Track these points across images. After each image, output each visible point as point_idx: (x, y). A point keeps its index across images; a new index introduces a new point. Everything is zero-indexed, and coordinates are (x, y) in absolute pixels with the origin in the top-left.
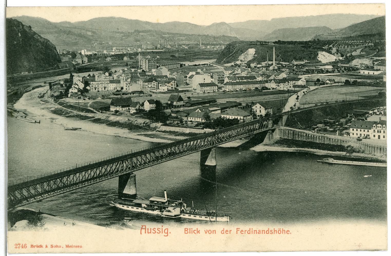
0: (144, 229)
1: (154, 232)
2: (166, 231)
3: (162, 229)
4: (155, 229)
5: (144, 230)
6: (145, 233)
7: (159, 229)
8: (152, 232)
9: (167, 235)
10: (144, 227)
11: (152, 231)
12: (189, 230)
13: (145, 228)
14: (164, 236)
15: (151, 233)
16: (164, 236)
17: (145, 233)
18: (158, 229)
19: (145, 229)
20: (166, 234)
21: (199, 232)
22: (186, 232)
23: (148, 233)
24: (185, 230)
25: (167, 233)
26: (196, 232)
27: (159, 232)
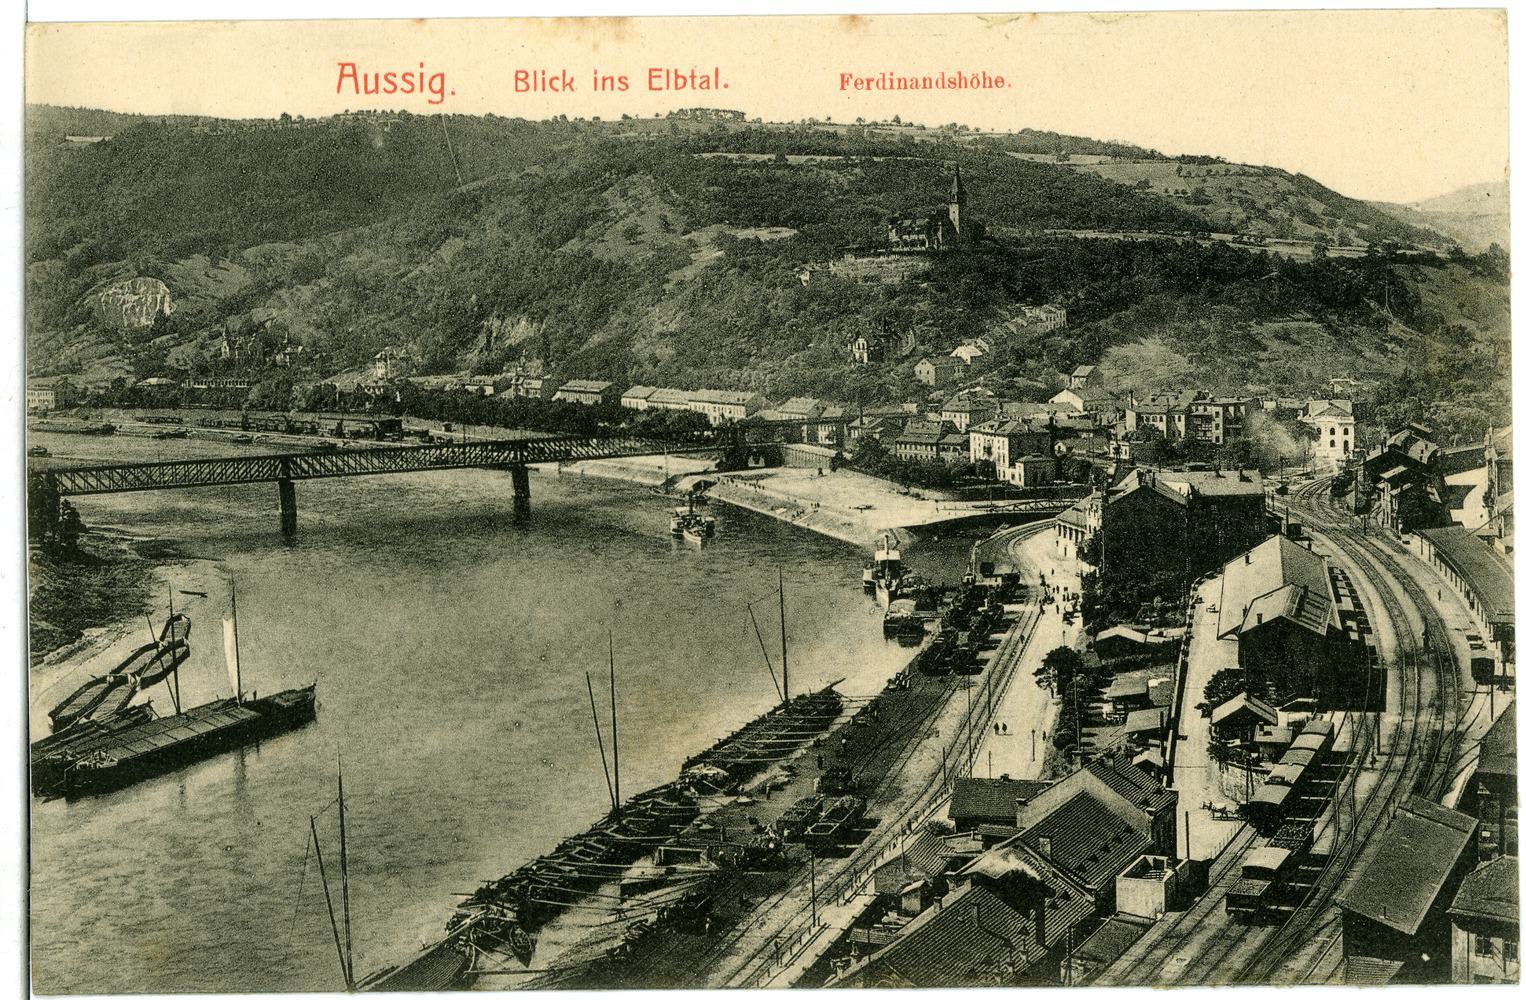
0: (349, 76)
1: (390, 88)
2: (436, 85)
3: (422, 75)
4: (395, 76)
5: (351, 79)
6: (357, 92)
7: (408, 78)
8: (381, 89)
9: (442, 100)
10: (348, 70)
11: (383, 84)
12: (530, 80)
13: (351, 72)
14: (430, 102)
15: (376, 90)
16: (430, 102)
17: (357, 92)
18: (404, 77)
19: (354, 75)
20: (437, 97)
21: (569, 84)
22: (521, 85)
23: (367, 92)
24: (517, 79)
25: (441, 91)
26: (558, 84)
27: (408, 87)
